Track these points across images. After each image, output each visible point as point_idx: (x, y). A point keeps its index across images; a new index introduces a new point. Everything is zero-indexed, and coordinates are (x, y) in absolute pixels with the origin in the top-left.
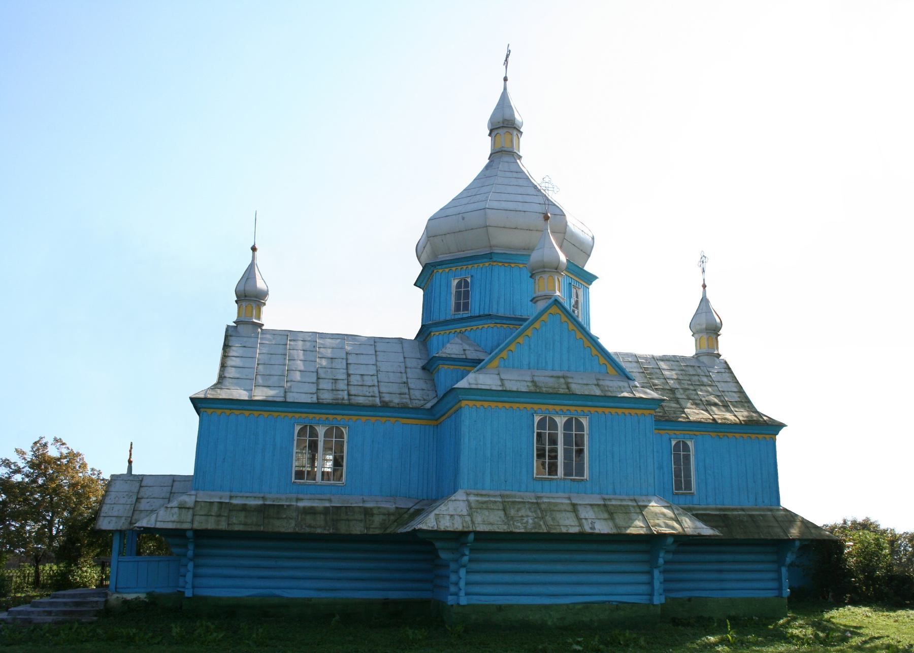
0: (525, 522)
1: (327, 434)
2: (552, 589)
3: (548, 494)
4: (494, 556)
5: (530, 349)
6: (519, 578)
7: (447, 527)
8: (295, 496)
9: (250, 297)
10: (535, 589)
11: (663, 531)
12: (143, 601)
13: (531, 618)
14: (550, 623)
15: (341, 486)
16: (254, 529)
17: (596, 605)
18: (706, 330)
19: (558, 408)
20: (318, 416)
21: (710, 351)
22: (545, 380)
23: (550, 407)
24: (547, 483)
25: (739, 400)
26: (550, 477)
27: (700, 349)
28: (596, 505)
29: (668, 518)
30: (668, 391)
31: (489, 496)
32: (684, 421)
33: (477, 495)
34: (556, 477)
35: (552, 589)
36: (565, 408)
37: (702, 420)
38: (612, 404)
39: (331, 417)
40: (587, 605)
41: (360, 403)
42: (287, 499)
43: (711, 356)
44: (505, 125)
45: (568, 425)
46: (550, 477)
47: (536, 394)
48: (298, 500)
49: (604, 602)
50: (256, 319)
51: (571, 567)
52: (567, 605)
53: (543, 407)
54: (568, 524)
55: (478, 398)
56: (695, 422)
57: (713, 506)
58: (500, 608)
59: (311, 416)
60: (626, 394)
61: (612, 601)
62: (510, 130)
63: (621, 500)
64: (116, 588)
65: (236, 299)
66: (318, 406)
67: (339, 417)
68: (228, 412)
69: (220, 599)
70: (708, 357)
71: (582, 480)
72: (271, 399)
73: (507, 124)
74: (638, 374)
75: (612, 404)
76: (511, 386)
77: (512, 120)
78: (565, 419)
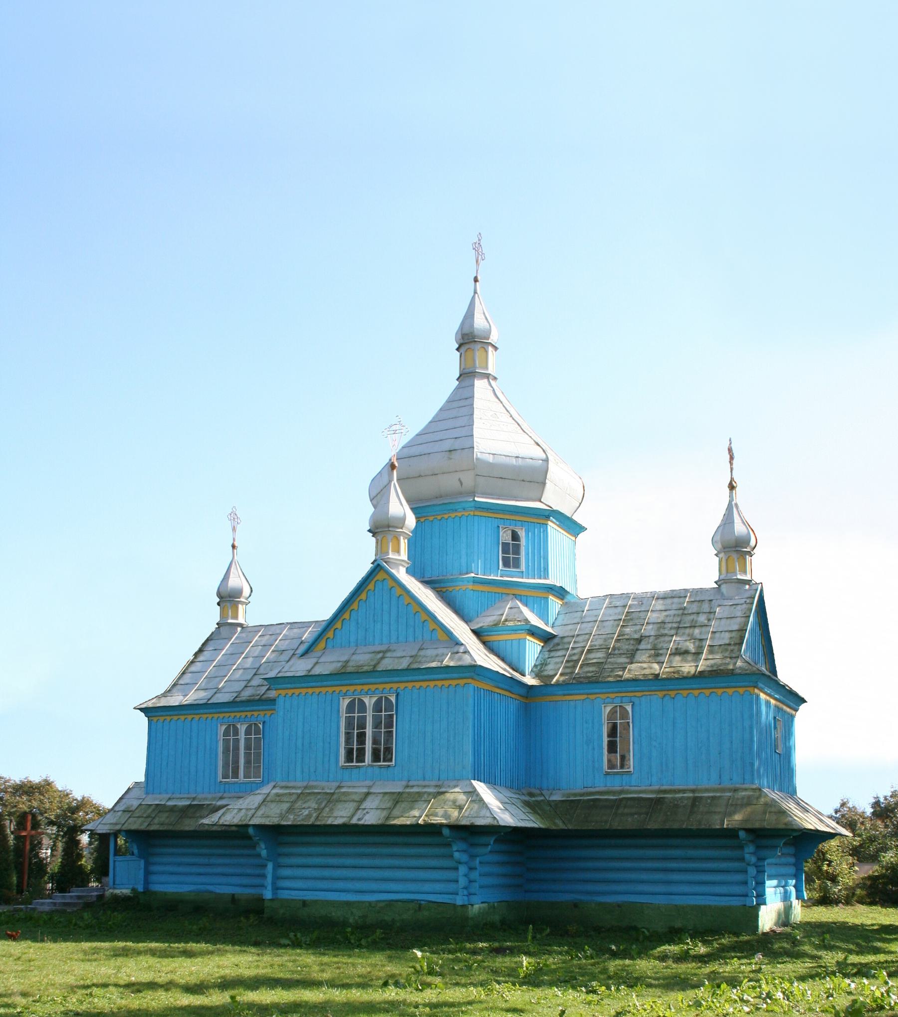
0: (305, 814)
1: (248, 732)
2: (359, 886)
3: (349, 784)
4: (304, 850)
5: (358, 623)
6: (327, 873)
7: (226, 821)
8: (220, 795)
9: (226, 597)
10: (341, 885)
11: (432, 822)
12: (129, 896)
13: (333, 914)
14: (351, 921)
15: (258, 783)
16: (170, 828)
17: (399, 903)
18: (724, 548)
19: (366, 688)
20: (238, 715)
21: (729, 576)
22: (362, 658)
23: (359, 688)
24: (355, 771)
25: (727, 642)
26: (357, 764)
27: (727, 572)
28: (390, 793)
29: (456, 806)
30: (632, 642)
31: (293, 787)
32: (614, 680)
33: (282, 787)
34: (363, 764)
35: (359, 886)
36: (373, 687)
37: (641, 677)
38: (421, 677)
39: (249, 714)
40: (390, 903)
41: (269, 698)
42: (214, 799)
43: (731, 582)
44: (466, 341)
45: (377, 707)
46: (357, 764)
47: (342, 675)
48: (221, 798)
49: (412, 901)
50: (232, 618)
51: (377, 862)
52: (370, 903)
53: (352, 688)
54: (340, 815)
55: (289, 686)
56: (627, 680)
57: (656, 787)
58: (304, 903)
59: (233, 715)
60: (434, 665)
61: (420, 900)
62: (472, 346)
63: (425, 786)
64: (114, 884)
65: (218, 600)
66: (233, 704)
67: (256, 714)
68: (169, 718)
69: (165, 893)
70: (727, 584)
71: (389, 766)
72: (196, 703)
73: (468, 339)
74: (612, 622)
75: (421, 677)
76: (317, 671)
77: (472, 333)
78: (374, 700)
